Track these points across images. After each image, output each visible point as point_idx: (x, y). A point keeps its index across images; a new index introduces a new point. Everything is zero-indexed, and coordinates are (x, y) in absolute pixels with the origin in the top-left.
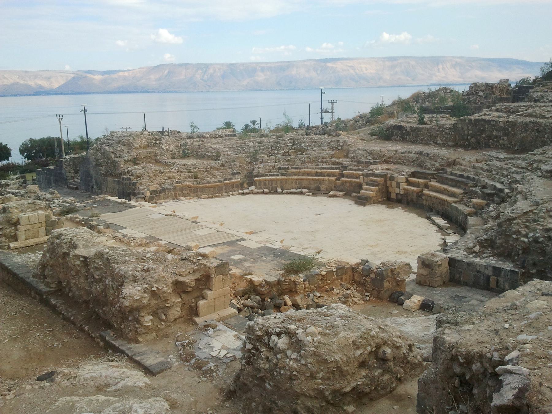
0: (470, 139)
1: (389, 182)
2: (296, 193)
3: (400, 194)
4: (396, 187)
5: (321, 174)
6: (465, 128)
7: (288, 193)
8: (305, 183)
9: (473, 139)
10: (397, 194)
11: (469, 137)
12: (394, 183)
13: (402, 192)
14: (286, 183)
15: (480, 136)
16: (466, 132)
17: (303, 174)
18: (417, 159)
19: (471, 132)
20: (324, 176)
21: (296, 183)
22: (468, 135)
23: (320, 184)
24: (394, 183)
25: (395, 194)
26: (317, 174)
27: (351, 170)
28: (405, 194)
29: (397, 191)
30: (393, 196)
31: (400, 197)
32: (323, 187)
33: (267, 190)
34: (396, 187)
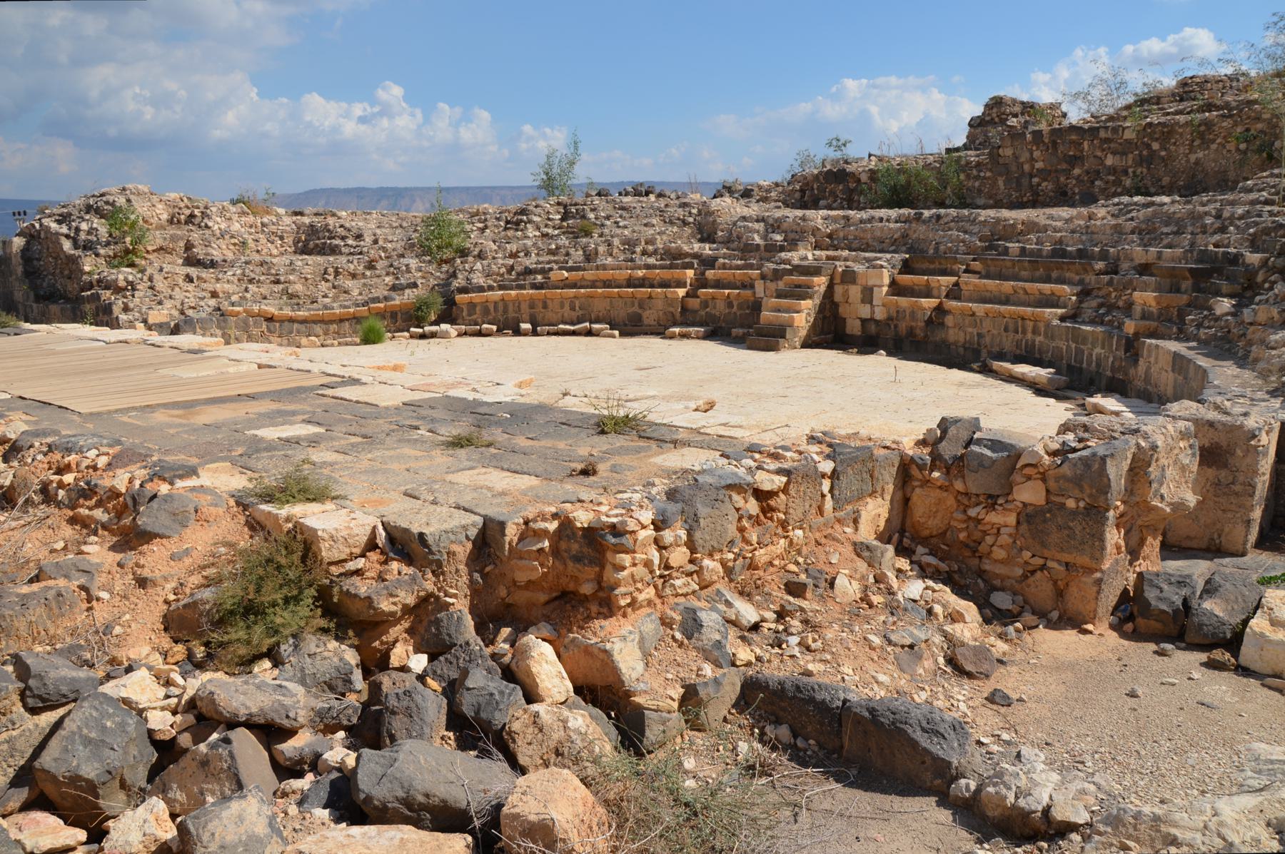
0: (1039, 185)
1: (839, 290)
2: (574, 333)
3: (872, 319)
4: (863, 301)
5: (642, 283)
6: (1025, 156)
7: (549, 334)
8: (600, 307)
9: (1044, 184)
10: (864, 321)
11: (1035, 180)
12: (855, 291)
13: (880, 314)
14: (545, 306)
15: (1068, 173)
16: (1027, 167)
17: (593, 284)
18: (905, 236)
19: (1039, 165)
20: (652, 286)
21: (573, 309)
22: (1031, 176)
23: (641, 307)
24: (855, 291)
25: (858, 323)
26: (630, 283)
27: (724, 267)
28: (890, 319)
29: (865, 311)
30: (854, 327)
31: (873, 328)
32: (649, 317)
33: (494, 328)
34: (863, 301)
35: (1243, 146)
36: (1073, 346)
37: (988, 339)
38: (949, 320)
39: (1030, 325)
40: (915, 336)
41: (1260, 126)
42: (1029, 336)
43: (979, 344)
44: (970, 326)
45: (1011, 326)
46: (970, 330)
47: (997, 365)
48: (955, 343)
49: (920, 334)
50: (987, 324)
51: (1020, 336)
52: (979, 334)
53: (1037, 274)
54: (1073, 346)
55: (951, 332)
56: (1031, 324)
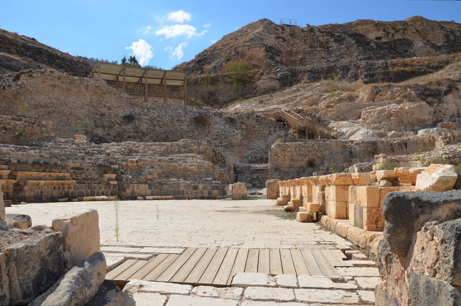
35: (4, 131)
36: (89, 190)
37: (46, 193)
38: (26, 188)
39: (66, 186)
40: (9, 196)
41: (10, 126)
42: (66, 190)
43: (41, 195)
44: (37, 189)
45: (57, 187)
46: (37, 191)
47: (85, 198)
48: (29, 197)
49: (11, 195)
50: (45, 188)
51: (61, 190)
52: (41, 192)
53: (40, 170)
54: (89, 190)
55: (27, 192)
56: (67, 186)
